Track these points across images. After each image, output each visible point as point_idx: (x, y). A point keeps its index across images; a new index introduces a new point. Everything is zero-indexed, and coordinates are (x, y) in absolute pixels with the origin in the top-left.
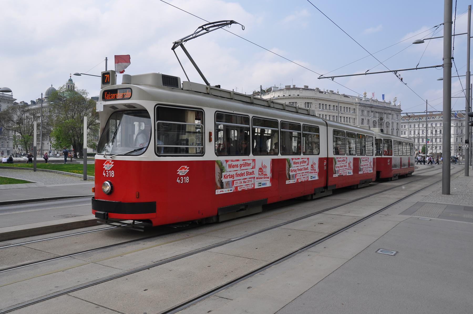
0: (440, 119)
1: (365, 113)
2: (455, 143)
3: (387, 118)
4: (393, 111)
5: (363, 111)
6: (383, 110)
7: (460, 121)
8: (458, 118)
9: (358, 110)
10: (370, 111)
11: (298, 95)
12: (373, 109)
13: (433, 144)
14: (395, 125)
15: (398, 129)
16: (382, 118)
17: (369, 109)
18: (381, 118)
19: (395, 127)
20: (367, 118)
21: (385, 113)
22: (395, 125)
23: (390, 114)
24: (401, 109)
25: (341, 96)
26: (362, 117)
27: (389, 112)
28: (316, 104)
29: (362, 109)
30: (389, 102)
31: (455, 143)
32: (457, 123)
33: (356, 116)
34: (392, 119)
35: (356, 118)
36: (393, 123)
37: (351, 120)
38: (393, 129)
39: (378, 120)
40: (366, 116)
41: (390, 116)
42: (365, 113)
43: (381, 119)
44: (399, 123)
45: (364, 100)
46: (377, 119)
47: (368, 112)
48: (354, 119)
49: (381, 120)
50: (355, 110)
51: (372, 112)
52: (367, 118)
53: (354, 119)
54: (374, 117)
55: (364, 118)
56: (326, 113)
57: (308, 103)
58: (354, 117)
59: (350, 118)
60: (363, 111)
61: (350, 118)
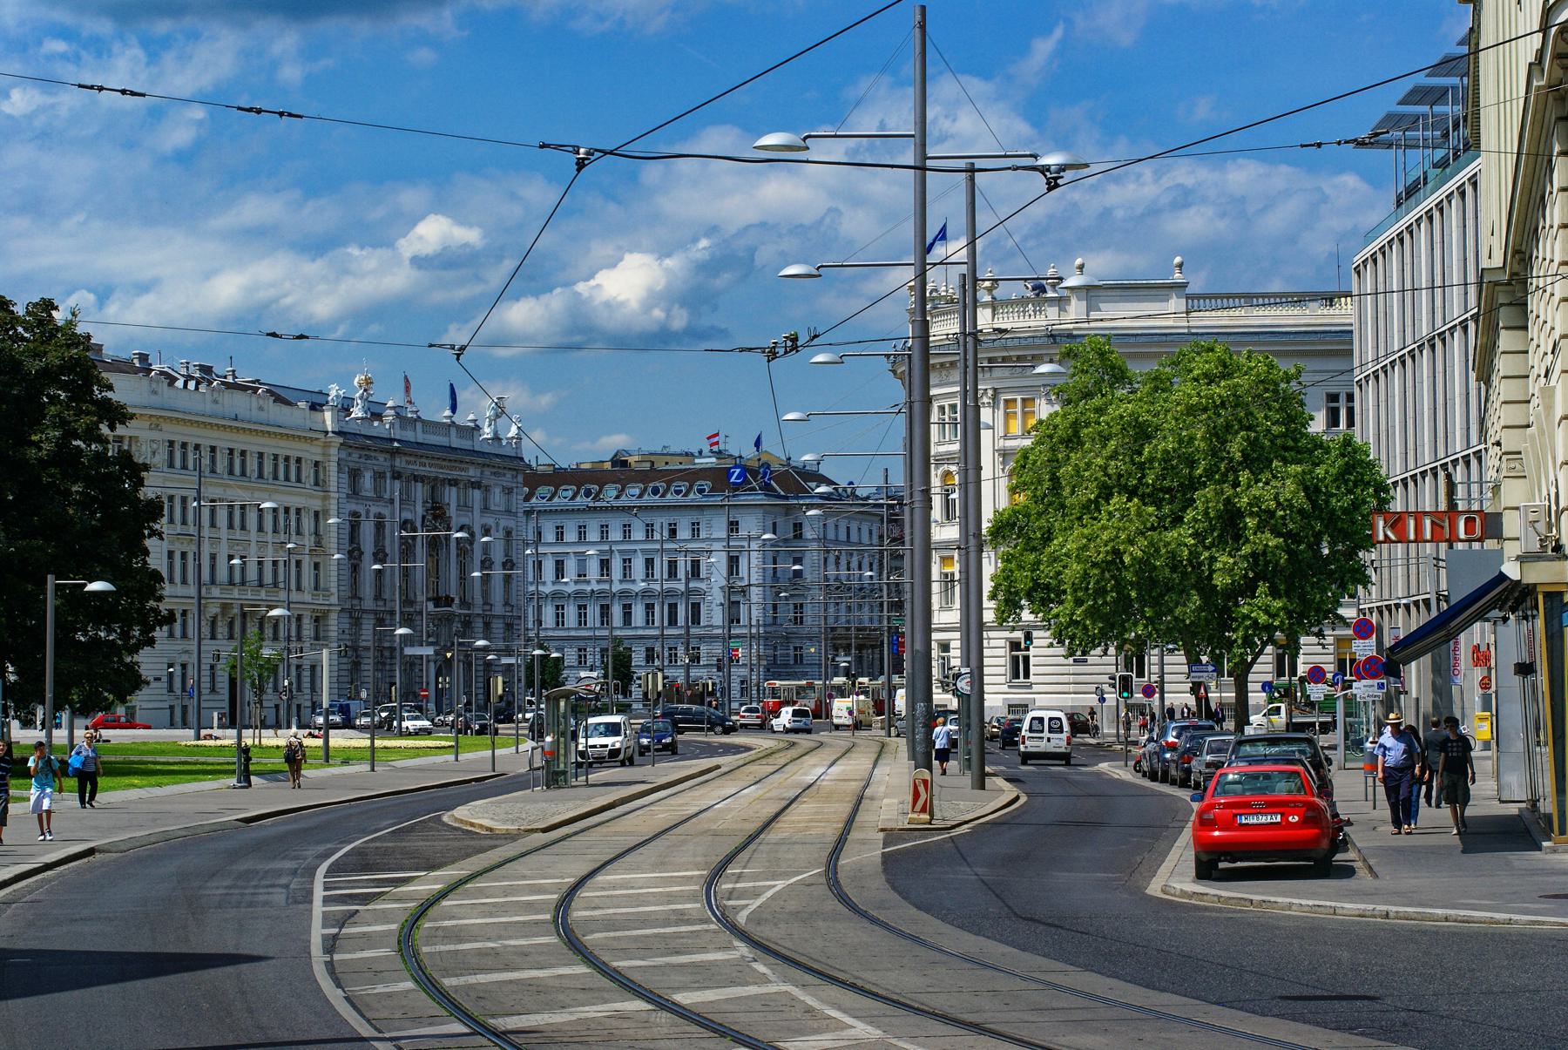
0: (693, 500)
2: (769, 629)
3: (464, 506)
4: (487, 472)
5: (355, 475)
6: (444, 463)
7: (788, 510)
8: (779, 497)
9: (333, 467)
10: (388, 475)
12: (400, 463)
13: (663, 635)
15: (511, 561)
16: (439, 508)
17: (382, 461)
18: (433, 508)
20: (374, 510)
21: (454, 483)
23: (476, 485)
24: (522, 459)
25: (261, 402)
26: (353, 507)
27: (473, 473)
28: (155, 446)
29: (352, 465)
30: (472, 424)
31: (769, 629)
32: (774, 524)
34: (486, 508)
39: (424, 517)
40: (367, 498)
41: (477, 494)
42: (367, 481)
43: (437, 513)
44: (514, 534)
45: (362, 419)
46: (420, 510)
47: (379, 476)
48: (316, 514)
49: (435, 517)
50: (321, 469)
51: (397, 476)
52: (374, 510)
53: (316, 514)
54: (406, 500)
55: (361, 509)
58: (316, 504)
59: (298, 511)
60: (355, 475)
61: (298, 511)
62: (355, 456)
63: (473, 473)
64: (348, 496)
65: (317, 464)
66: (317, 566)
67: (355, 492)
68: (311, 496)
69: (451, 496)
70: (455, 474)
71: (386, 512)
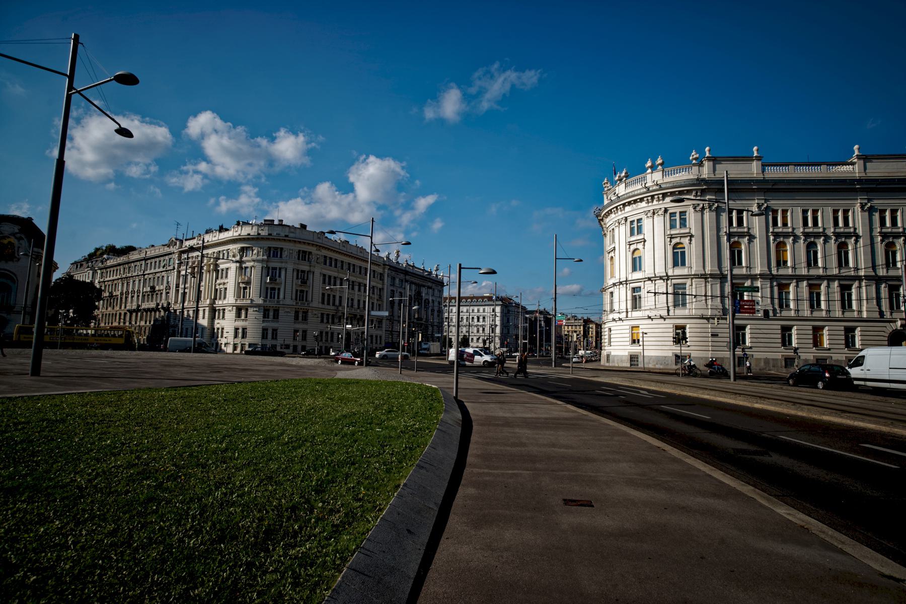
1: (397, 281)
5: (393, 279)
11: (286, 236)
12: (408, 277)
14: (436, 304)
17: (402, 276)
19: (436, 309)
22: (436, 304)
23: (429, 288)
26: (392, 288)
27: (430, 284)
33: (383, 284)
34: (433, 295)
35: (383, 289)
36: (433, 301)
37: (376, 290)
38: (433, 310)
42: (397, 281)
46: (413, 293)
55: (395, 290)
56: (336, 274)
57: (304, 252)
58: (380, 286)
60: (393, 279)
62: (394, 273)
63: (430, 284)
64: (391, 285)
65: (381, 274)
66: (379, 305)
67: (393, 285)
68: (378, 283)
69: (424, 291)
70: (424, 284)
71: (403, 291)
